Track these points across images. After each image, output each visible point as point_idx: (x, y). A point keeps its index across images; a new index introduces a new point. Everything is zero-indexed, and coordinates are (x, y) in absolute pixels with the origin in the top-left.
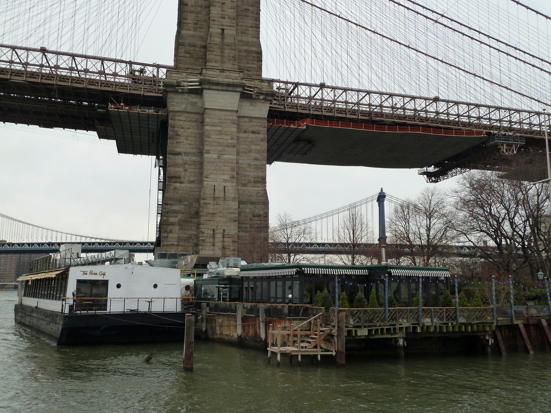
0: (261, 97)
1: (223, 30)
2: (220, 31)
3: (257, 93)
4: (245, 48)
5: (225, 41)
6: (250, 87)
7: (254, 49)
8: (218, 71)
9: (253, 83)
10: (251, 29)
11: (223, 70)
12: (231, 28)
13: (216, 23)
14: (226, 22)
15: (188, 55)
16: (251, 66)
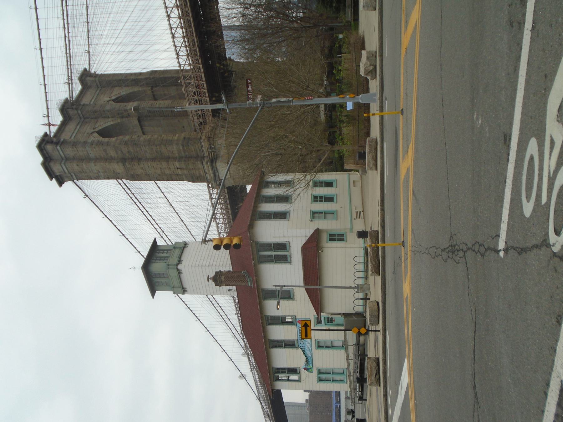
0: (213, 146)
1: (177, 168)
2: (179, 170)
3: (211, 149)
4: (183, 153)
5: (184, 168)
6: (209, 154)
7: (181, 148)
8: (207, 175)
9: (205, 151)
10: (168, 149)
11: (205, 173)
12: (175, 164)
13: (175, 171)
14: (172, 167)
15: (199, 179)
16: (193, 150)
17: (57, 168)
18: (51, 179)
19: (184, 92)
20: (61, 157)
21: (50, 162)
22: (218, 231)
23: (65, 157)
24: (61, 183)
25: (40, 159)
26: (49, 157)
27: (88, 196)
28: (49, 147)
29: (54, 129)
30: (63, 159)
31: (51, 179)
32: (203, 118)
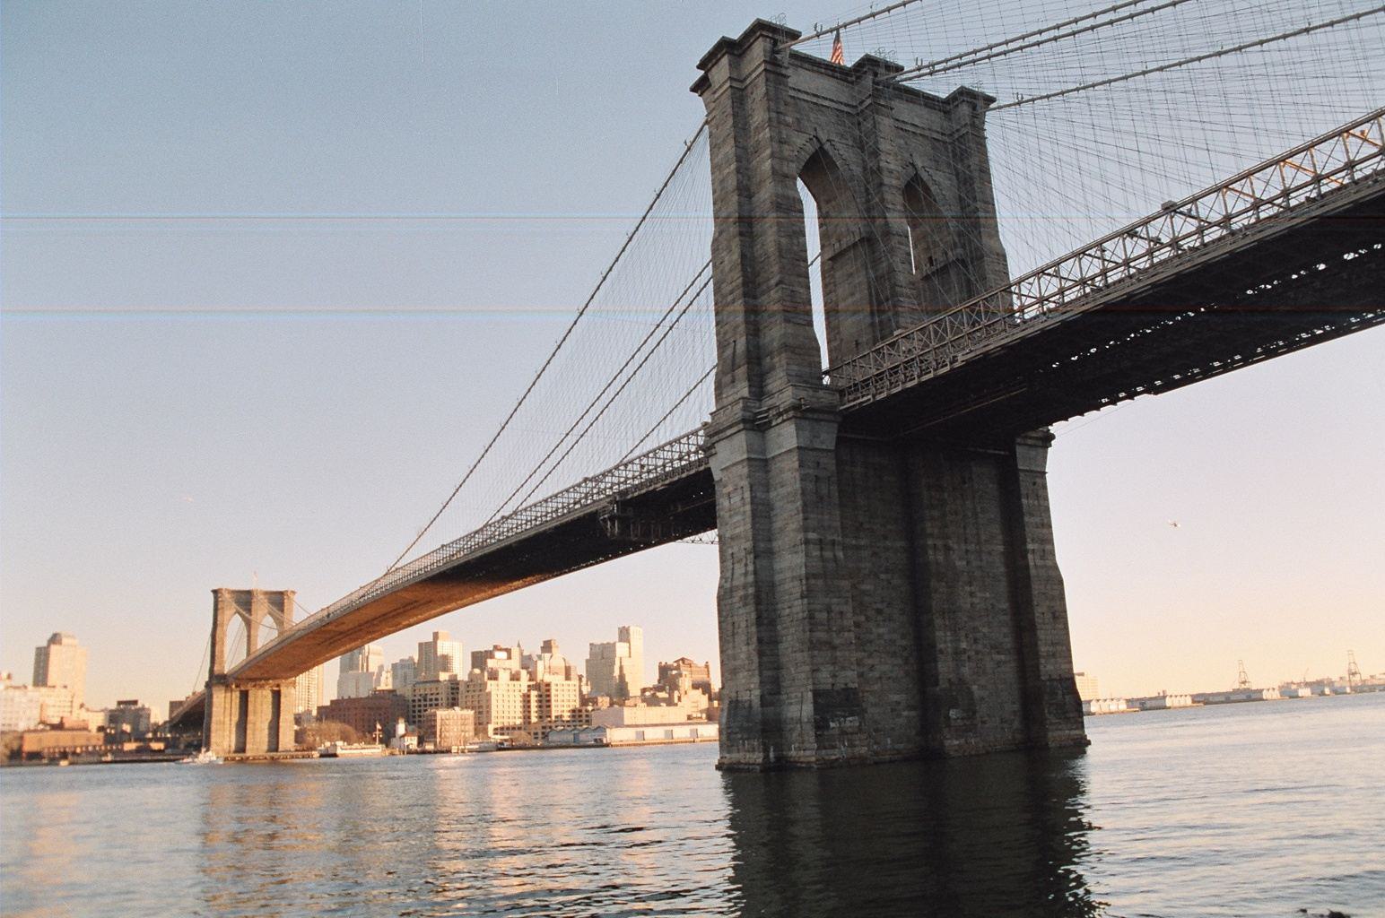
17: (721, 72)
18: (699, 67)
19: (896, 333)
20: (745, 79)
21: (731, 54)
22: (665, 445)
23: (746, 87)
24: (701, 87)
25: (735, 35)
26: (744, 52)
27: (689, 149)
28: (759, 50)
29: (821, 50)
30: (742, 81)
31: (699, 67)
32: (850, 387)
